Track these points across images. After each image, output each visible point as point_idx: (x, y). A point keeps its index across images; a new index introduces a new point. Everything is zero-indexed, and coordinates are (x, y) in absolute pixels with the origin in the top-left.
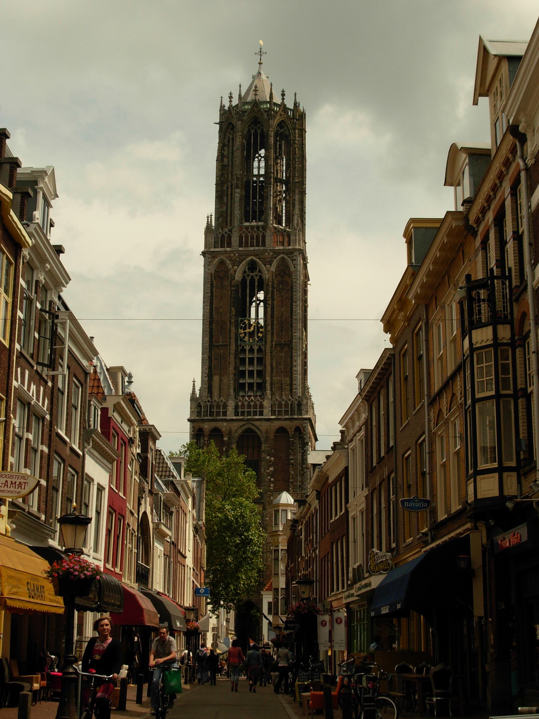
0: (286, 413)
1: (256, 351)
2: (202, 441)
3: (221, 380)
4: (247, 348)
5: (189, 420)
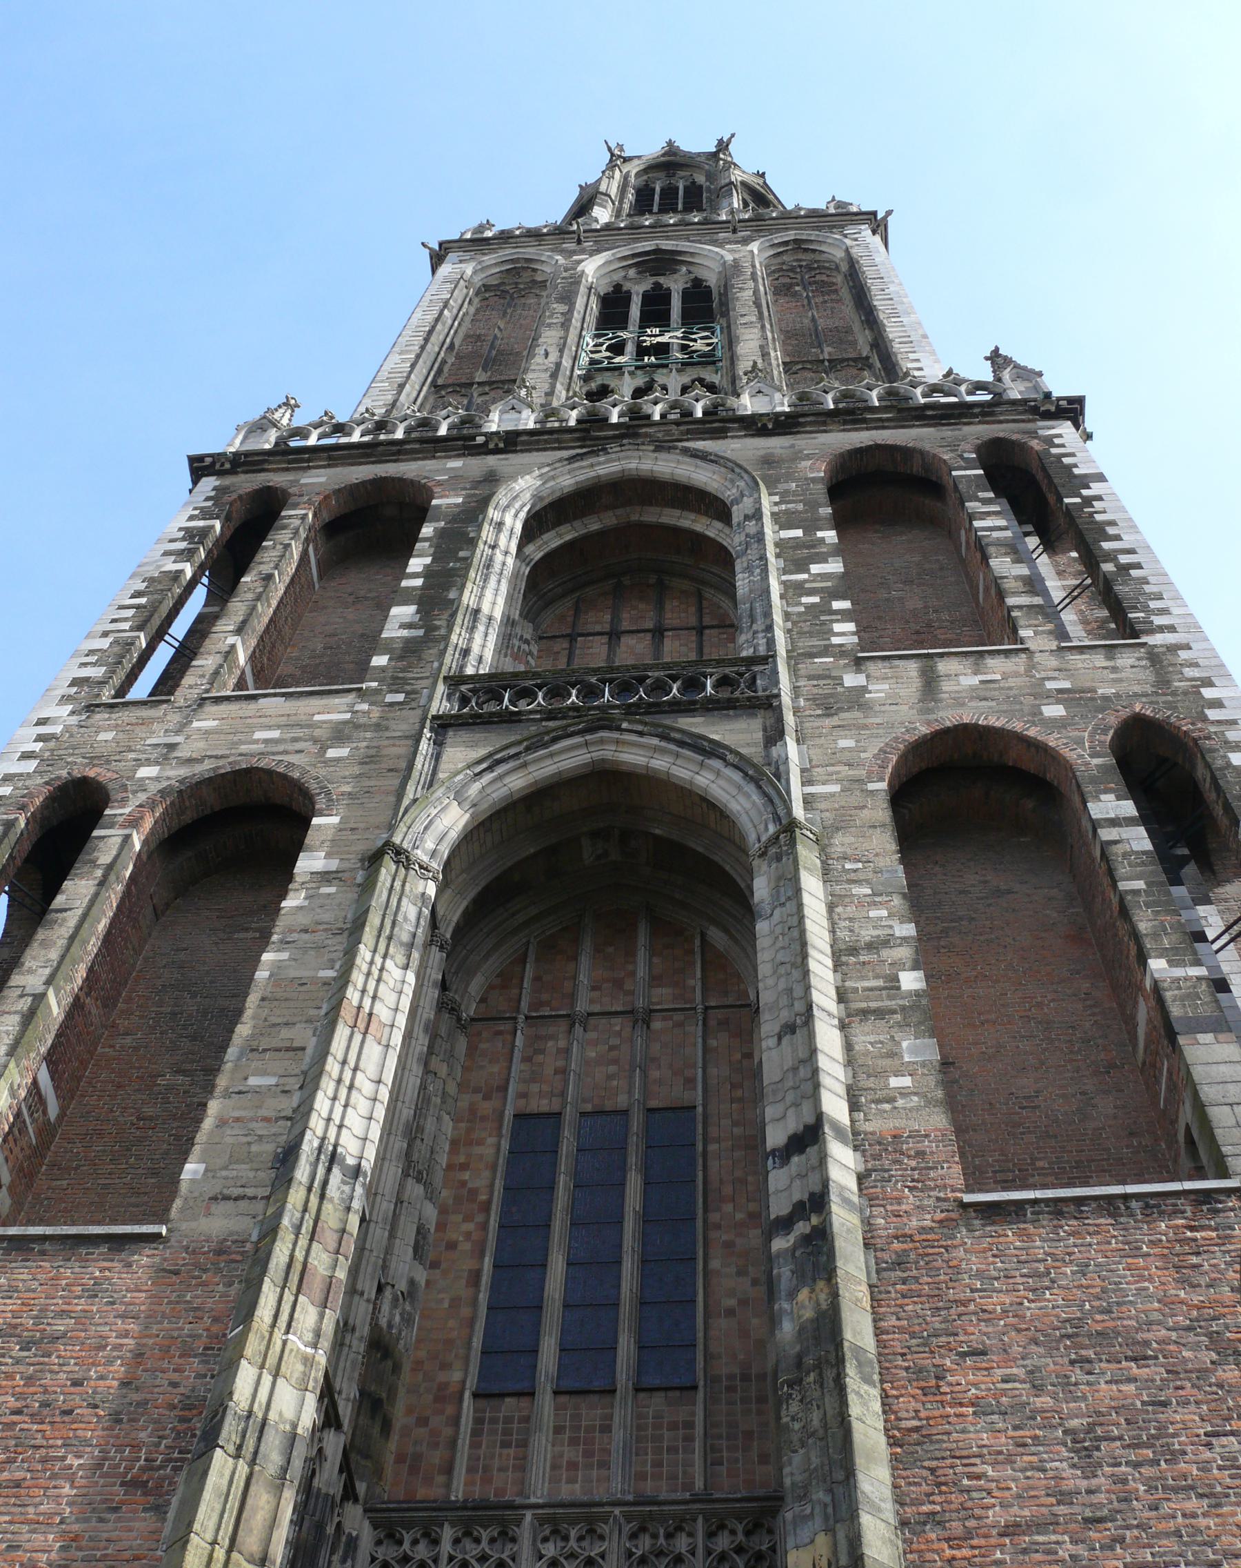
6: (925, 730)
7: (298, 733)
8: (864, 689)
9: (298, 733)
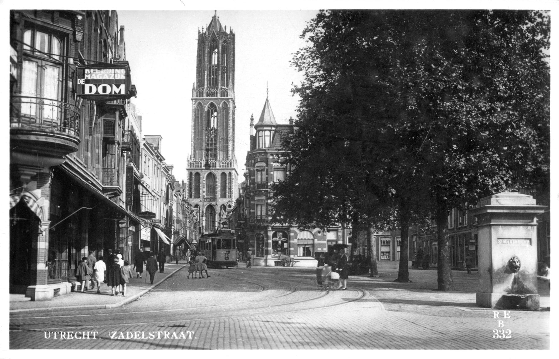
0: (226, 167)
5: (187, 169)
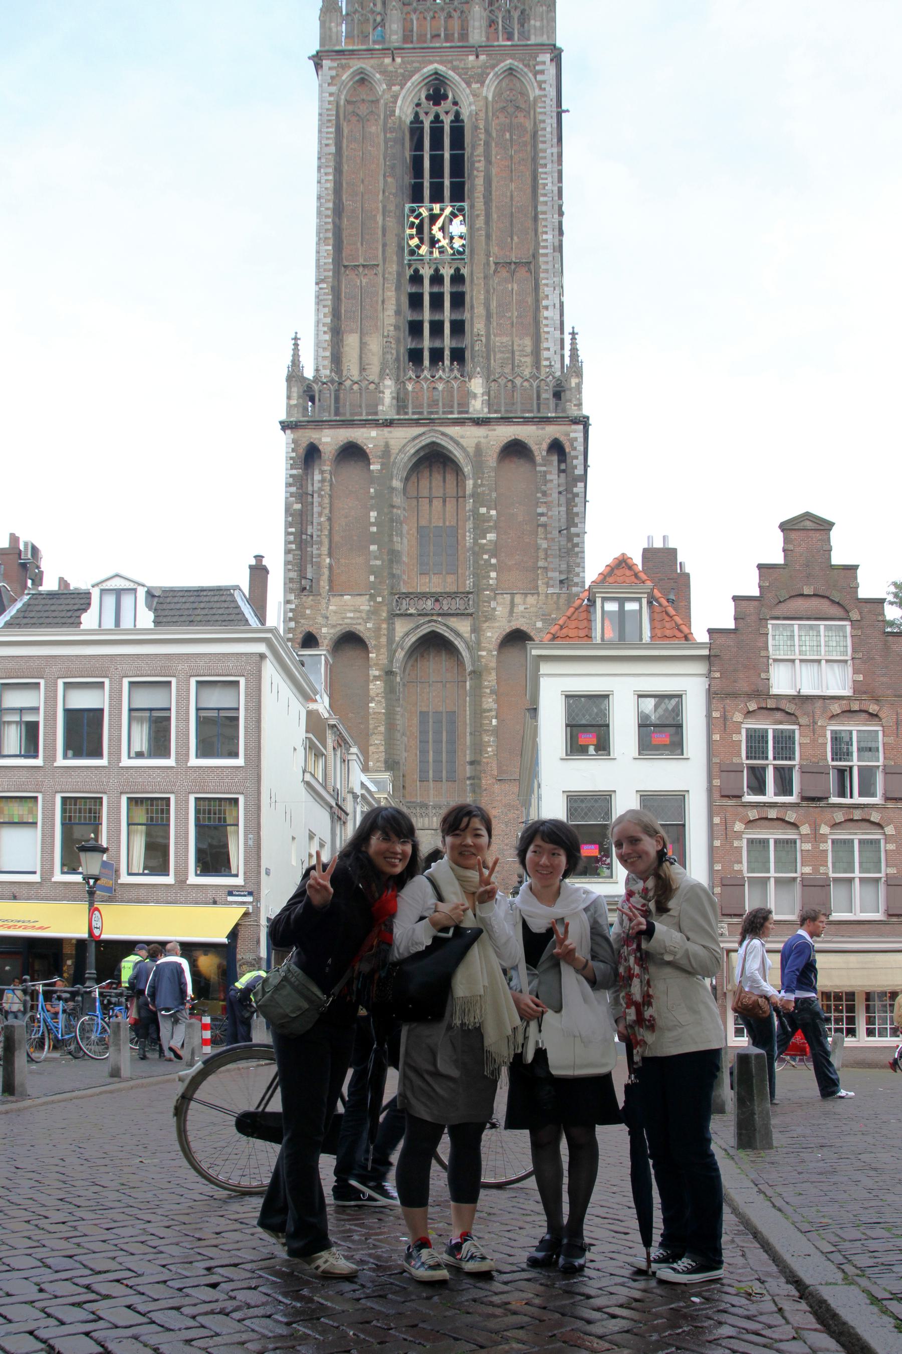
1: (447, 281)
2: (317, 477)
3: (363, 345)
4: (427, 272)
6: (508, 630)
7: (358, 615)
8: (494, 609)
9: (358, 615)
